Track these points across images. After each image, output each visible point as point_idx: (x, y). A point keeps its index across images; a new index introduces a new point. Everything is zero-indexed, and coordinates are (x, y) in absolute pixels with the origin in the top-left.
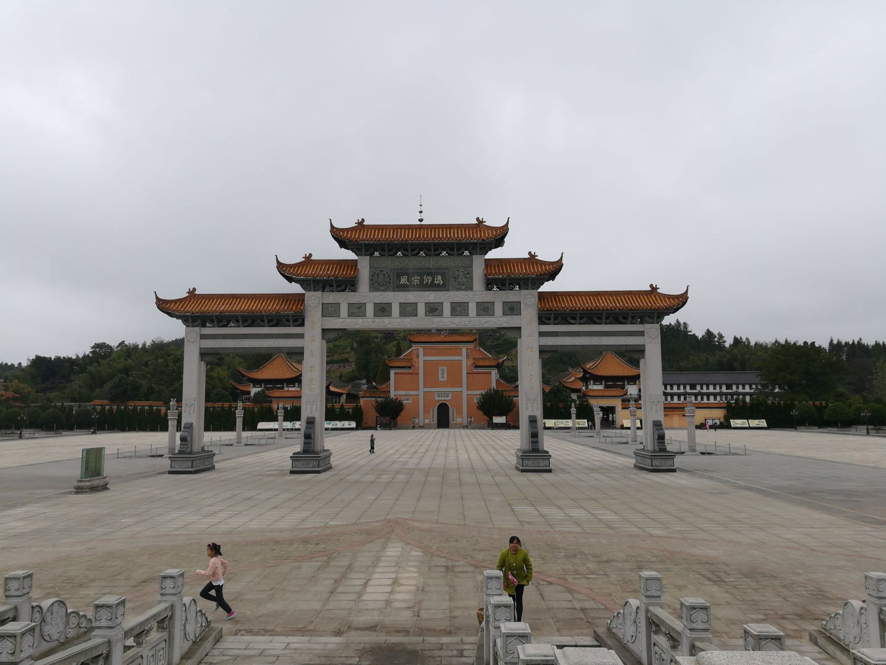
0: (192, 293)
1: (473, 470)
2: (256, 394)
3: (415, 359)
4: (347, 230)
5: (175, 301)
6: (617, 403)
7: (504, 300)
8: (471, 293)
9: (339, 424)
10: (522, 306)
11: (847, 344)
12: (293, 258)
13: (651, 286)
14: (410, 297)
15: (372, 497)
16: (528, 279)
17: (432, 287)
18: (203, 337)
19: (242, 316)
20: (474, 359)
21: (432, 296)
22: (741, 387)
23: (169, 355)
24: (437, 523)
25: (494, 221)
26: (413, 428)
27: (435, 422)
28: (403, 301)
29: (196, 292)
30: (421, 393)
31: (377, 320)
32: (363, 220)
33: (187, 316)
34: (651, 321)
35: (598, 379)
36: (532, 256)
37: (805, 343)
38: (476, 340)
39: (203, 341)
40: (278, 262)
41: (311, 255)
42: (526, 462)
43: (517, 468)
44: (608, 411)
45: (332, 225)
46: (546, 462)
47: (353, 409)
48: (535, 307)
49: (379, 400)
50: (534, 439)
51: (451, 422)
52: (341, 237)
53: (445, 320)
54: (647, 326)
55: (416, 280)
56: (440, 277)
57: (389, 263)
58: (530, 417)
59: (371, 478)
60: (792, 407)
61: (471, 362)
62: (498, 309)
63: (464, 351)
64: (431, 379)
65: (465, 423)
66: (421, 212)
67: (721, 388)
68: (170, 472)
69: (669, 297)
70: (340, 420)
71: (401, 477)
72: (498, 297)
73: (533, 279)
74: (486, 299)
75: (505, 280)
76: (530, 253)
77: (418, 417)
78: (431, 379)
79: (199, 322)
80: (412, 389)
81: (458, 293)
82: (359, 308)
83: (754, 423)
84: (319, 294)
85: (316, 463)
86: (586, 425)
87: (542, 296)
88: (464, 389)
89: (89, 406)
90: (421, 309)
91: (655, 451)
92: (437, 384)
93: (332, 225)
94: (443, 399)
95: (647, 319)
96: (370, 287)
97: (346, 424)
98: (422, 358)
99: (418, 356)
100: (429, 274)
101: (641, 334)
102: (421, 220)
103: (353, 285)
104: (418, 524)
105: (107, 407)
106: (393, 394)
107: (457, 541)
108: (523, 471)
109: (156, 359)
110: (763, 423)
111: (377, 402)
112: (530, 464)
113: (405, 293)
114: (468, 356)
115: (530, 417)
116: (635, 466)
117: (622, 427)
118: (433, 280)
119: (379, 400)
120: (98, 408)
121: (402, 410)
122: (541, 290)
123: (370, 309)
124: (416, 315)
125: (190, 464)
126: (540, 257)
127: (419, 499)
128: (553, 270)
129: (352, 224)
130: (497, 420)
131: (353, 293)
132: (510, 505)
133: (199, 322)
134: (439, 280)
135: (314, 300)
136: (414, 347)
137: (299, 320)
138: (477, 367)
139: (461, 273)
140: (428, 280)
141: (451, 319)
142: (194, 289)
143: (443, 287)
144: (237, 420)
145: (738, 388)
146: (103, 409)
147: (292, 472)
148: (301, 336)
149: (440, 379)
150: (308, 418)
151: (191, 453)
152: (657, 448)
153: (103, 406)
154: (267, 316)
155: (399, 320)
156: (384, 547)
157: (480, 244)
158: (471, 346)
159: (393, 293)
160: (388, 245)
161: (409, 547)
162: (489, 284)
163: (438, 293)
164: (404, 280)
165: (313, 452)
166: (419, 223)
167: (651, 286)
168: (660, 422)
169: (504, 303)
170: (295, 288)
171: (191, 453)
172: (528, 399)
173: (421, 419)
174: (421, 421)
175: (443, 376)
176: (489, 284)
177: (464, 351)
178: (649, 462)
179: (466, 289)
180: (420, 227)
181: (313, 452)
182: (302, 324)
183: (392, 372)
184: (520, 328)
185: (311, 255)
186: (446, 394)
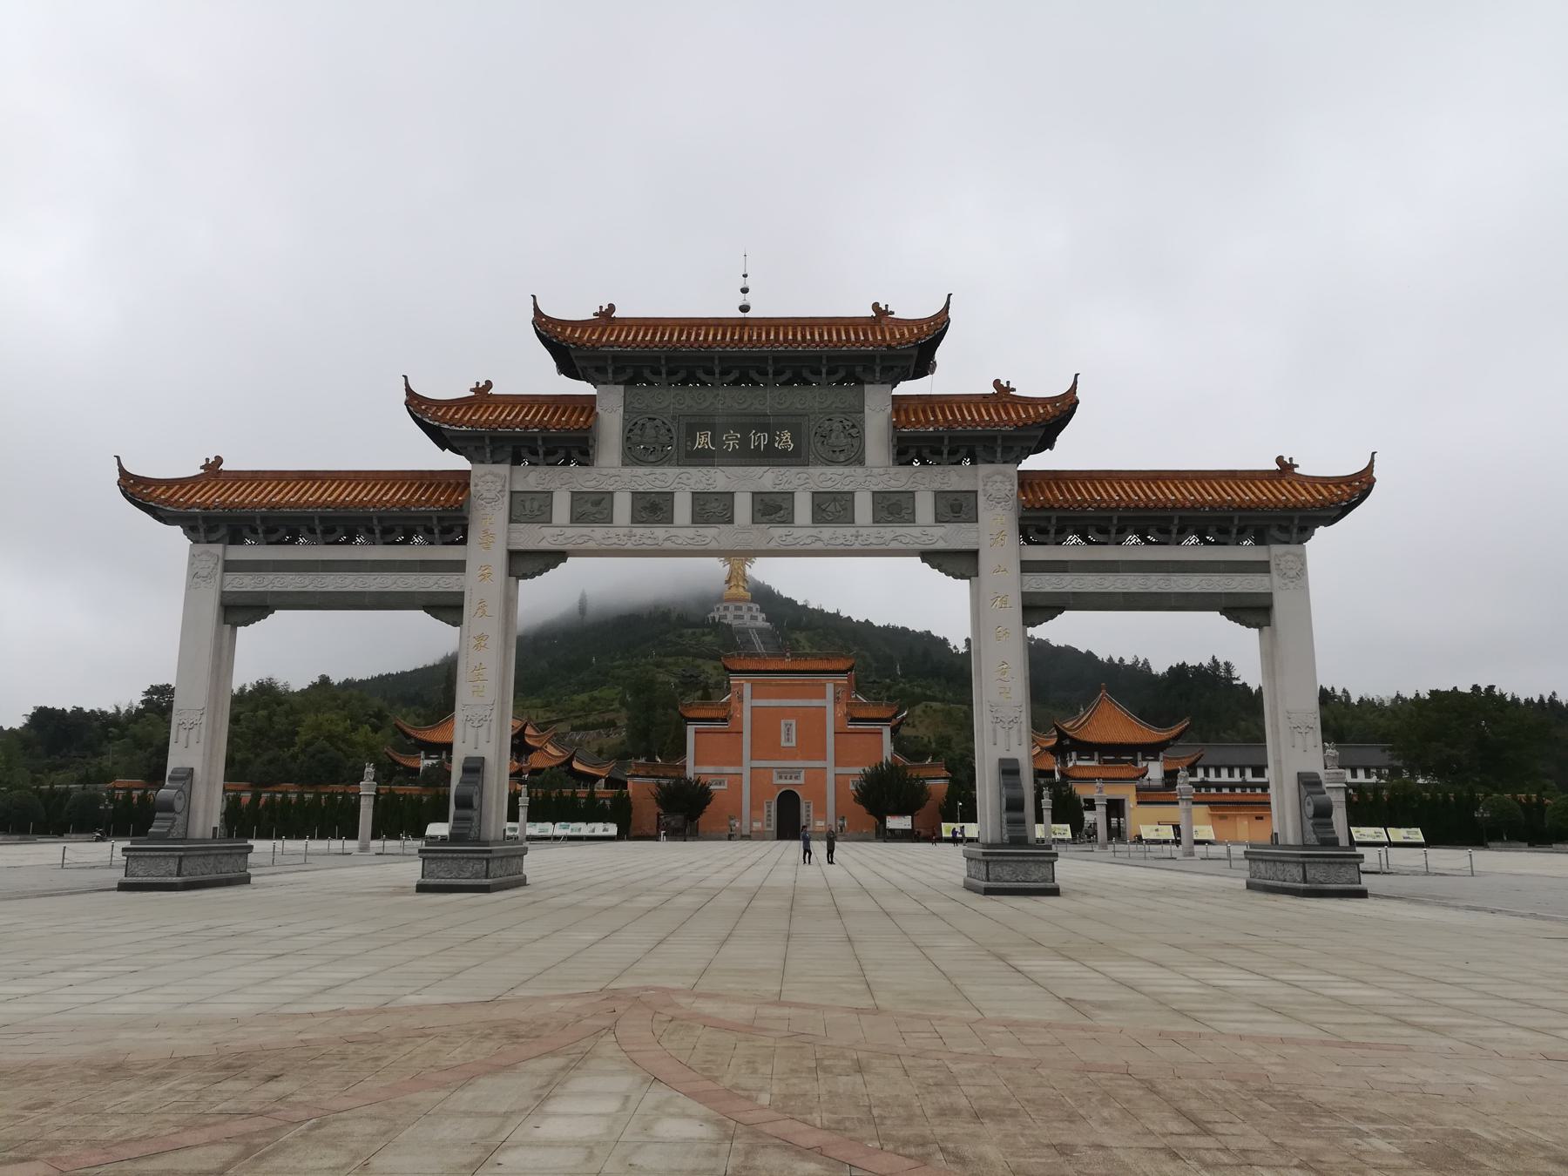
0: (213, 469)
1: (864, 891)
2: (427, 769)
4: (574, 324)
5: (169, 483)
6: (1128, 793)
7: (937, 486)
8: (859, 470)
9: (584, 829)
10: (981, 499)
11: (1529, 702)
12: (449, 386)
13: (1280, 460)
14: (718, 478)
15: (590, 937)
16: (994, 438)
17: (770, 456)
18: (230, 566)
19: (323, 519)
21: (768, 478)
23: (279, 704)
24: (779, 1003)
25: (912, 306)
26: (730, 838)
27: (773, 828)
28: (700, 488)
29: (223, 467)
31: (640, 531)
32: (612, 308)
33: (194, 517)
34: (1284, 537)
35: (1086, 749)
36: (1003, 390)
37: (1476, 688)
38: (850, 670)
39: (229, 577)
40: (409, 390)
41: (489, 384)
42: (996, 870)
43: (969, 887)
44: (1115, 808)
45: (536, 309)
46: (1044, 870)
47: (614, 800)
48: (1013, 502)
49: (664, 782)
50: (1016, 815)
52: (563, 342)
53: (797, 532)
54: (1277, 549)
55: (731, 442)
56: (787, 435)
57: (669, 400)
58: (1002, 761)
59: (613, 900)
60: (1473, 804)
62: (925, 507)
63: (830, 689)
64: (766, 745)
66: (745, 291)
68: (123, 887)
69: (1326, 481)
70: (588, 822)
71: (685, 901)
72: (926, 483)
73: (1007, 438)
74: (894, 486)
75: (941, 439)
76: (997, 383)
78: (766, 745)
79: (223, 531)
81: (830, 471)
82: (597, 503)
83: (1398, 834)
84: (504, 469)
85: (480, 867)
86: (1069, 835)
87: (1028, 481)
89: (103, 789)
90: (743, 508)
91: (1305, 846)
92: (777, 752)
93: (536, 309)
94: (787, 782)
95: (1274, 532)
96: (624, 455)
97: (599, 829)
98: (748, 703)
99: (741, 698)
100: (763, 427)
101: (1263, 567)
102: (745, 309)
103: (585, 453)
104: (709, 1008)
105: (136, 793)
106: (691, 771)
107: (859, 1068)
108: (988, 892)
109: (255, 710)
110: (1417, 835)
111: (659, 785)
112: (1006, 875)
113: (704, 470)
114: (837, 699)
115: (1002, 761)
116: (1250, 886)
117: (1139, 839)
118: (772, 441)
119: (664, 782)
120: (120, 794)
122: (1021, 467)
123: (622, 507)
124: (731, 521)
125: (173, 867)
126: (1022, 390)
127: (723, 943)
128: (1053, 417)
129: (587, 314)
130: (894, 823)
131: (583, 469)
132: (1001, 958)
133: (223, 531)
134: (785, 440)
135: (492, 483)
136: (734, 680)
137: (453, 528)
138: (854, 720)
139: (836, 425)
140: (759, 439)
141: (814, 531)
142: (219, 460)
143: (795, 458)
144: (363, 802)
146: (129, 797)
147: (421, 888)
148: (459, 566)
149: (783, 744)
150: (467, 759)
151: (184, 839)
152: (1312, 839)
153: (129, 790)
154: (380, 519)
155: (691, 532)
156: (544, 1096)
157: (883, 358)
158: (843, 680)
159: (677, 470)
160: (668, 359)
161: (658, 1094)
162: (907, 449)
163: (783, 470)
164: (703, 441)
165: (478, 841)
166: (742, 315)
167: (1280, 460)
168: (1316, 776)
169: (939, 495)
170: (458, 462)
171: (184, 839)
172: (998, 720)
173: (746, 822)
174: (744, 825)
175: (789, 741)
176: (907, 449)
177: (830, 689)
178: (1296, 872)
179: (848, 462)
180: (743, 324)
181: (478, 841)
182: (464, 542)
183: (691, 730)
184: (974, 554)
185: (489, 384)
186: (794, 773)
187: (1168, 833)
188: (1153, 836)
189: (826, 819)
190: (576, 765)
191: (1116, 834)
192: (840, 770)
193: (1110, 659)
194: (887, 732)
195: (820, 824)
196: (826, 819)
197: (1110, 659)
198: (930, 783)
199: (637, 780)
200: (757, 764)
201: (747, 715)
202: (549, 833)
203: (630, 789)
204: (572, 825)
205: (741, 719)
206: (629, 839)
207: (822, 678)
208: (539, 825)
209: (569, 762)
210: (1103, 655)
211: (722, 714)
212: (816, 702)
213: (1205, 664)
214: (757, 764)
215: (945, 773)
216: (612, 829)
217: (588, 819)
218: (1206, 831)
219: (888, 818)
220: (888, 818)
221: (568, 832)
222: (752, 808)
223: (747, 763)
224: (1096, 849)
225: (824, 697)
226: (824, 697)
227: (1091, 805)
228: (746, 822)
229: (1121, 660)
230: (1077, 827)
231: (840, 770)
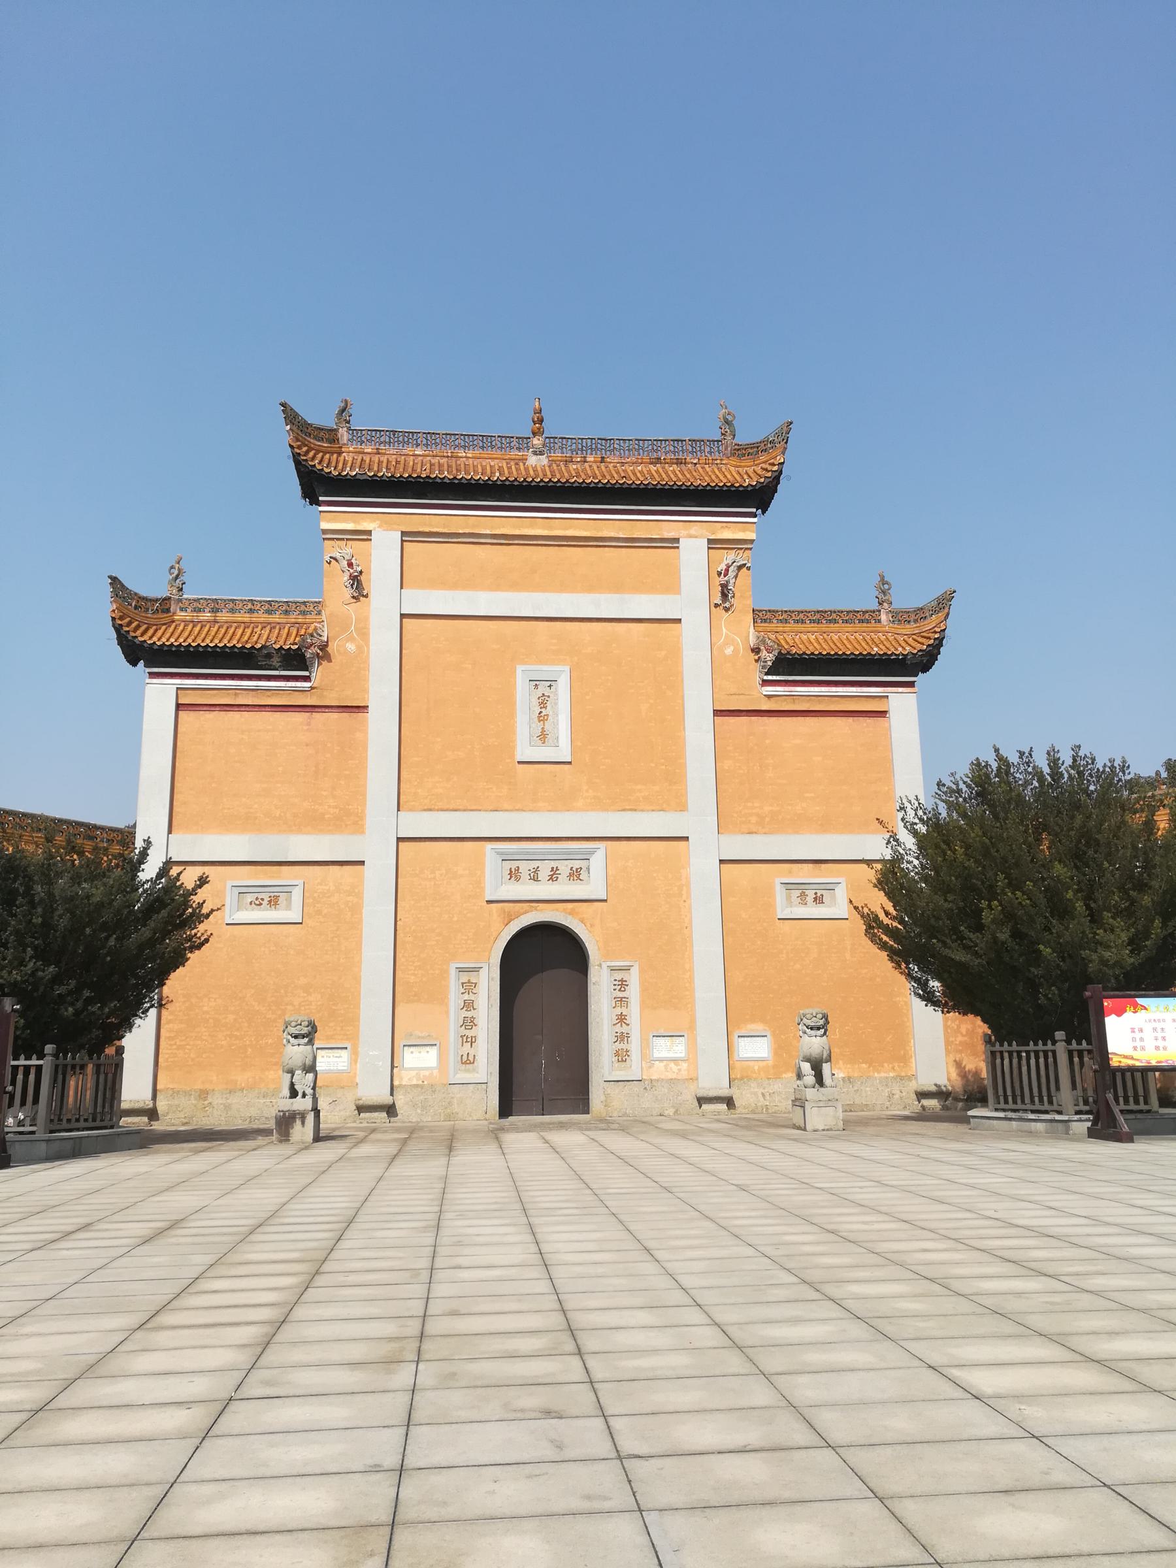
20: (761, 616)
30: (375, 848)
61: (741, 631)
64: (455, 749)
78: (455, 749)
80: (313, 822)
88: (697, 819)
92: (494, 772)
94: (542, 897)
98: (385, 600)
138: (789, 665)
195: (664, 1049)
205: (361, 659)
223: (382, 825)
225: (670, 584)
226: (670, 584)
228: (375, 1050)
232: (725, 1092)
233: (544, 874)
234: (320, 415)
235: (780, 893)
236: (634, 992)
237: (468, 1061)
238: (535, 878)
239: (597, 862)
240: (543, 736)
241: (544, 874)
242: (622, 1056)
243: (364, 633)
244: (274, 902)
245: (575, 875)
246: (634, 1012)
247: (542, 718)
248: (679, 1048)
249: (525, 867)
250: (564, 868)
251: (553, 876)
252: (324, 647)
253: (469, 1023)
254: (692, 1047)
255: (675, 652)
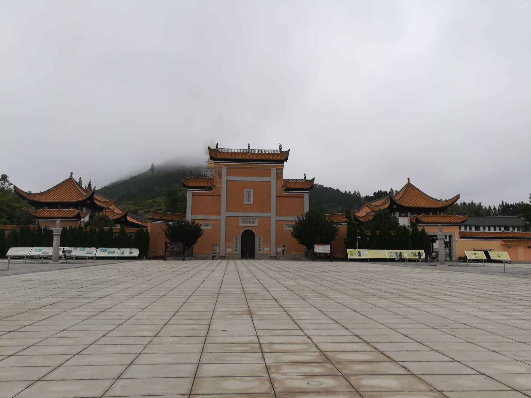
3: (217, 179)
9: (117, 252)
11: (511, 205)
22: (487, 228)
26: (213, 258)
47: (137, 233)
49: (171, 223)
51: (257, 251)
65: (273, 253)
67: (470, 229)
70: (119, 247)
77: (218, 244)
80: (213, 214)
88: (273, 214)
94: (248, 225)
97: (126, 252)
98: (224, 178)
99: (220, 175)
106: (189, 217)
111: (167, 225)
117: (463, 259)
119: (171, 223)
121: (200, 236)
130: (319, 249)
138: (288, 189)
145: (484, 229)
149: (246, 202)
173: (222, 248)
175: (249, 200)
183: (189, 194)
186: (252, 220)
187: (481, 256)
188: (473, 257)
189: (270, 246)
190: (129, 219)
191: (450, 257)
192: (279, 218)
193: (346, 192)
194: (306, 196)
195: (267, 249)
196: (270, 246)
197: (346, 192)
198: (339, 225)
199: (153, 222)
200: (229, 214)
201: (224, 185)
202: (93, 254)
203: (149, 228)
204: (109, 250)
205: (220, 189)
206: (148, 258)
207: (270, 165)
208: (87, 249)
209: (125, 217)
210: (343, 190)
211: (209, 185)
212: (265, 179)
213: (388, 191)
214: (229, 214)
215: (345, 220)
216: (136, 252)
217: (119, 247)
218: (505, 256)
219: (316, 246)
220: (316, 246)
221: (105, 254)
222: (226, 240)
224: (438, 264)
225: (270, 176)
226: (270, 176)
227: (434, 239)
229: (350, 192)
230: (429, 252)
231: (279, 218)
232: (275, 255)
233: (248, 222)
234: (214, 147)
235: (285, 226)
236: (262, 241)
237: (236, 250)
238: (247, 223)
239: (257, 221)
240: (249, 200)
241: (248, 222)
242: (259, 250)
243: (221, 184)
244: (207, 226)
245: (253, 222)
246: (262, 243)
247: (248, 197)
248: (268, 249)
249: (245, 221)
250: (251, 221)
251: (250, 223)
252: (214, 186)
253: (236, 245)
254: (270, 249)
255: (270, 186)
